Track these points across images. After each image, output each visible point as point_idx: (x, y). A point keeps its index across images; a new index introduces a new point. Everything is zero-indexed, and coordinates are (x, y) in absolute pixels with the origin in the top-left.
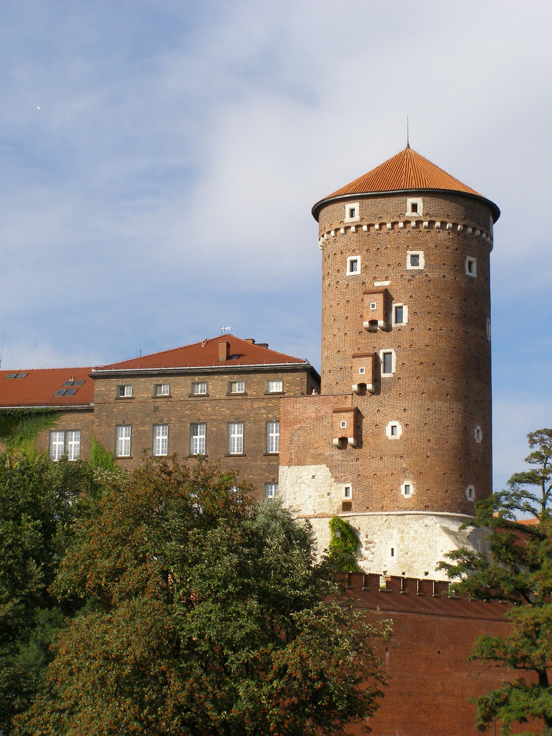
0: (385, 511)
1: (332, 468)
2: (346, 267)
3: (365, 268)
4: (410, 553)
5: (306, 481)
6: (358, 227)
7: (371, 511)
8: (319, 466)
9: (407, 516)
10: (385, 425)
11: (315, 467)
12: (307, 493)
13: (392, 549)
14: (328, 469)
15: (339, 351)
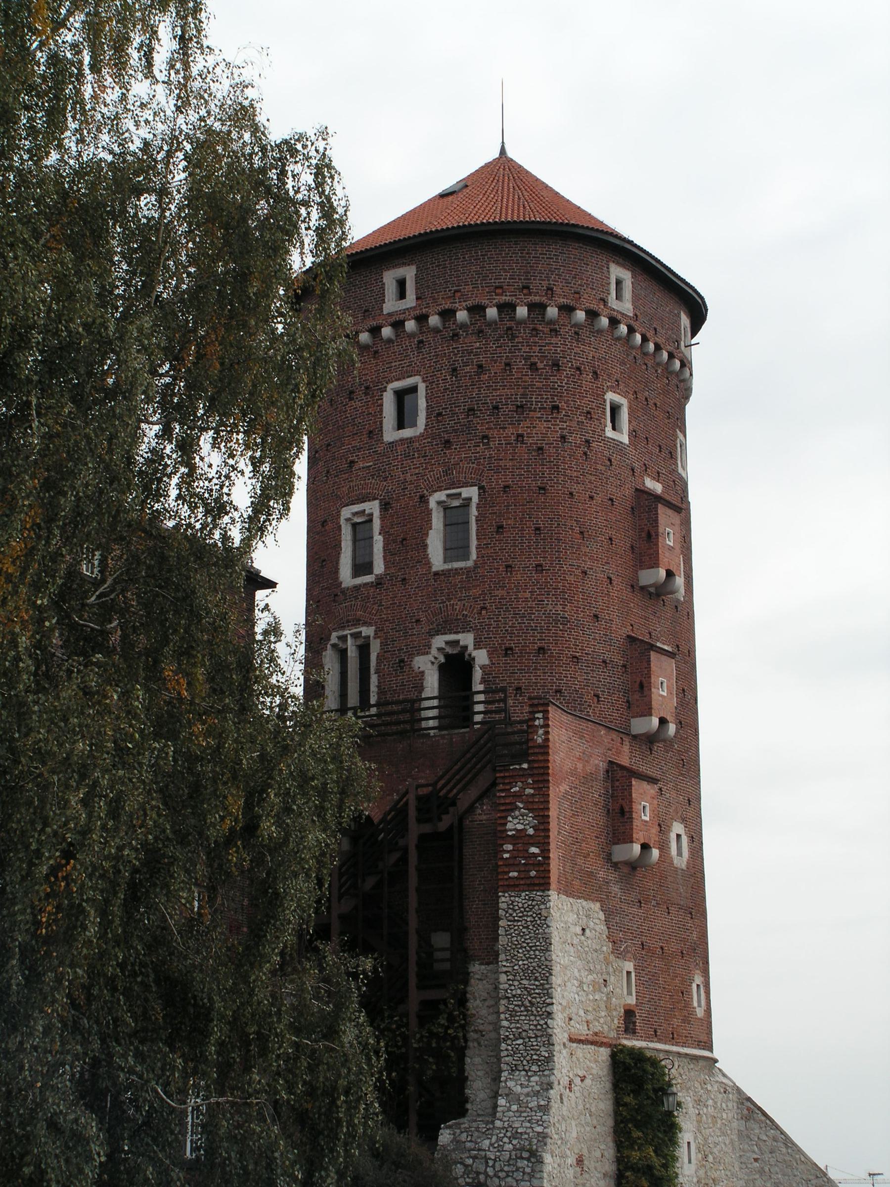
0: (677, 1044)
1: (609, 914)
2: (604, 413)
3: (633, 434)
4: (710, 1158)
5: (576, 941)
6: (631, 330)
7: (660, 1041)
8: (593, 906)
9: (702, 1063)
10: (669, 827)
11: (585, 903)
12: (577, 975)
13: (689, 1143)
14: (602, 916)
15: (596, 616)
